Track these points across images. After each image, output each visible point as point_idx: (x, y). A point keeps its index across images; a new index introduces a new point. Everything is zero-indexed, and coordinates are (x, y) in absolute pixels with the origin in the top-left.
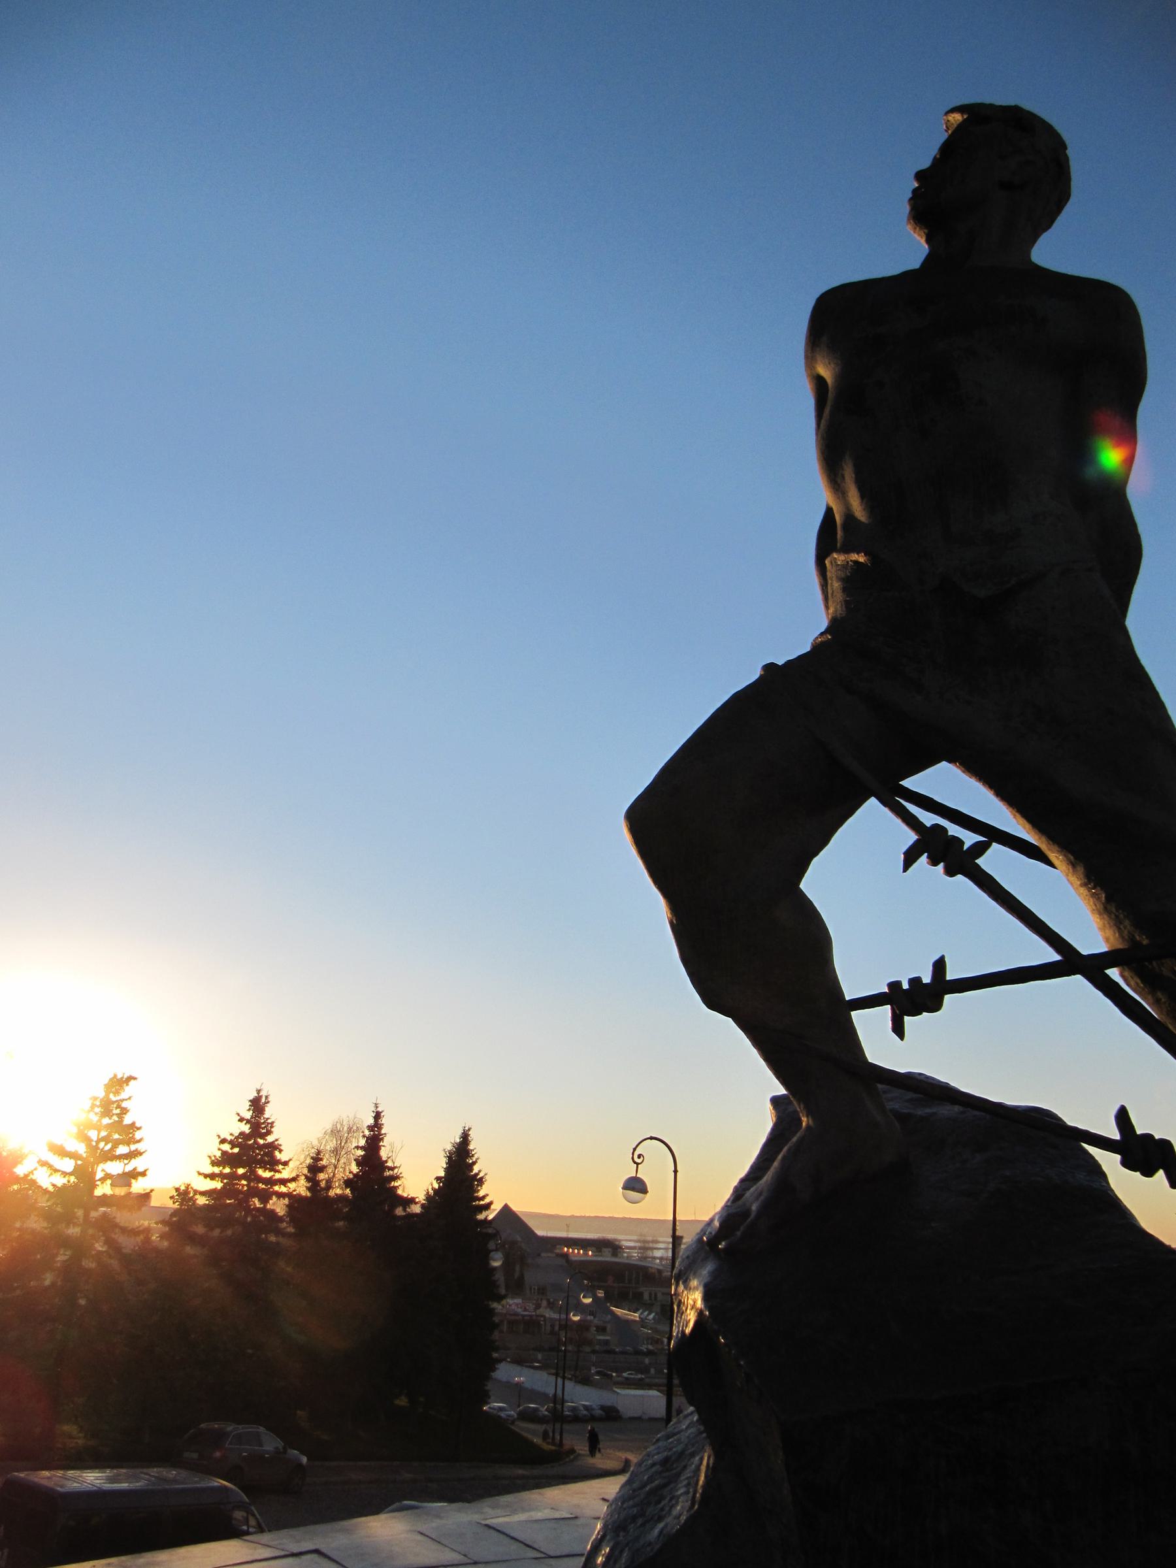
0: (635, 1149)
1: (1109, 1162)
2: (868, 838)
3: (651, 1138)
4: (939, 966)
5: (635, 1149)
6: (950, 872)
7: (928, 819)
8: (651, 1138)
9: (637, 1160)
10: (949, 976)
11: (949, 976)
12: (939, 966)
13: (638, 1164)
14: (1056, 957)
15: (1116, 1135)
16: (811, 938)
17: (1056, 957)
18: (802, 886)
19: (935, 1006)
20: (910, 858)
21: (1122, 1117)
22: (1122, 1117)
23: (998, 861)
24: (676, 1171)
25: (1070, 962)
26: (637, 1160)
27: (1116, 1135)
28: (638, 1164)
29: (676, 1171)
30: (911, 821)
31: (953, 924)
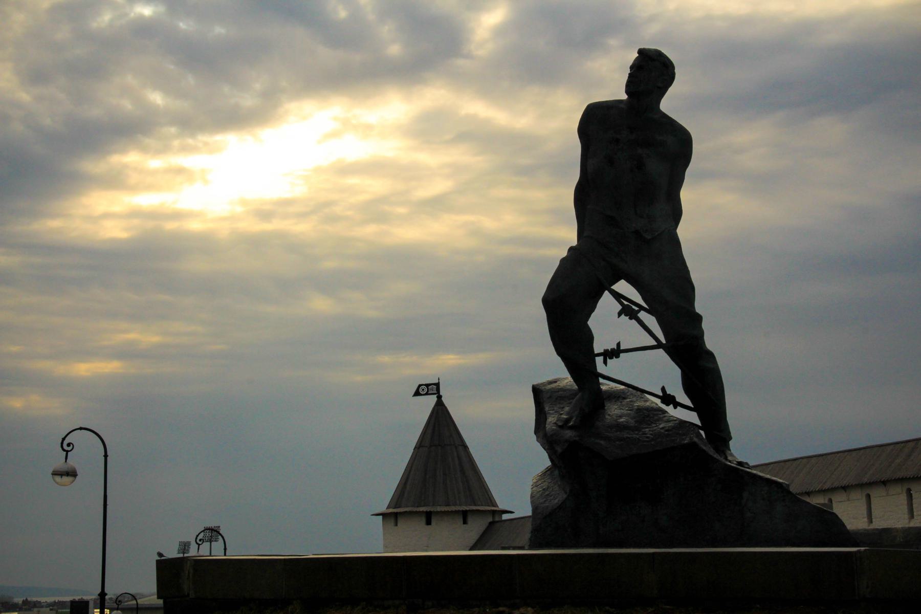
0: (64, 439)
1: (658, 401)
2: (607, 304)
3: (81, 429)
4: (619, 344)
5: (64, 439)
6: (631, 319)
7: (626, 303)
8: (81, 429)
9: (66, 447)
10: (622, 348)
11: (622, 348)
12: (619, 344)
13: (67, 452)
14: (654, 343)
15: (661, 394)
16: (590, 338)
17: (654, 343)
18: (589, 323)
19: (618, 357)
20: (620, 314)
21: (663, 389)
22: (663, 389)
23: (643, 315)
24: (106, 456)
25: (659, 345)
26: (66, 447)
27: (661, 394)
28: (67, 452)
29: (106, 456)
30: (621, 304)
31: (630, 333)
